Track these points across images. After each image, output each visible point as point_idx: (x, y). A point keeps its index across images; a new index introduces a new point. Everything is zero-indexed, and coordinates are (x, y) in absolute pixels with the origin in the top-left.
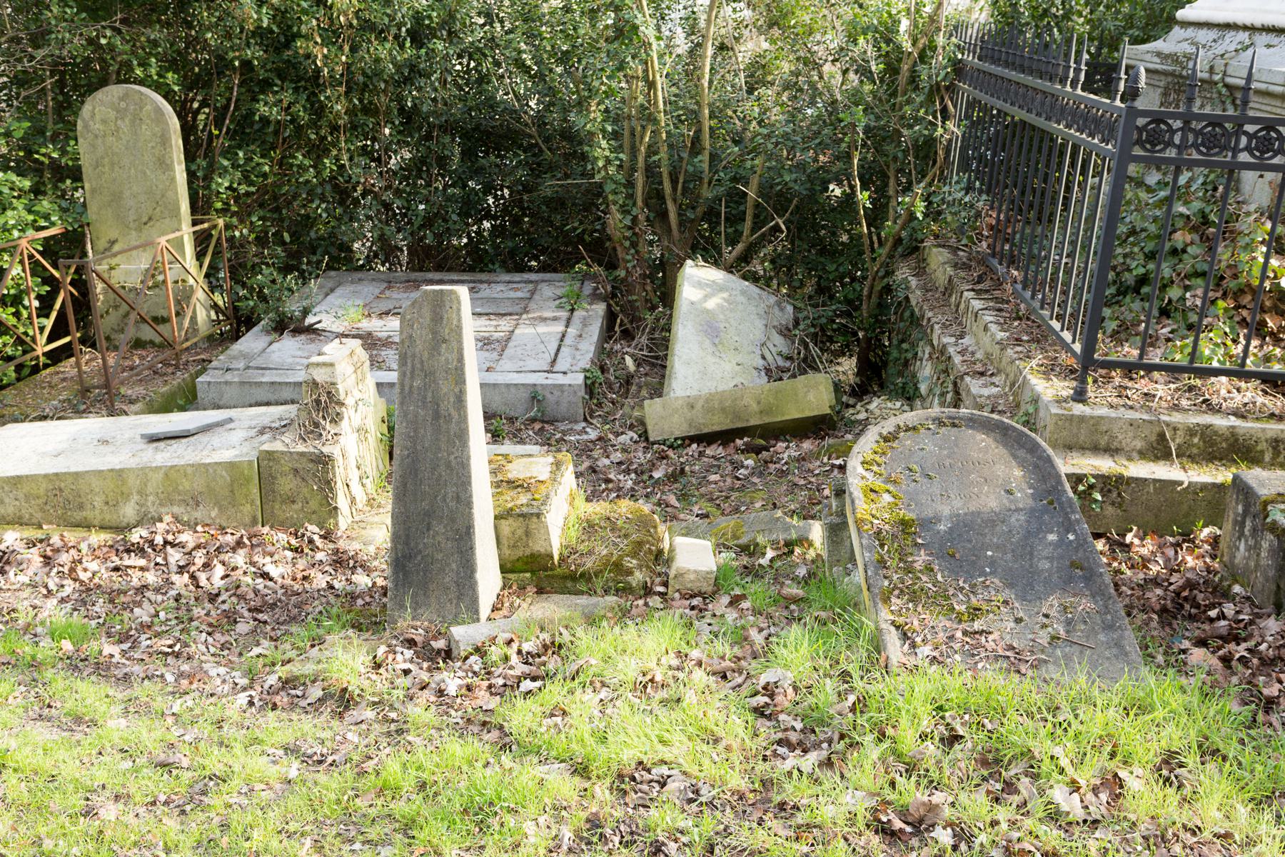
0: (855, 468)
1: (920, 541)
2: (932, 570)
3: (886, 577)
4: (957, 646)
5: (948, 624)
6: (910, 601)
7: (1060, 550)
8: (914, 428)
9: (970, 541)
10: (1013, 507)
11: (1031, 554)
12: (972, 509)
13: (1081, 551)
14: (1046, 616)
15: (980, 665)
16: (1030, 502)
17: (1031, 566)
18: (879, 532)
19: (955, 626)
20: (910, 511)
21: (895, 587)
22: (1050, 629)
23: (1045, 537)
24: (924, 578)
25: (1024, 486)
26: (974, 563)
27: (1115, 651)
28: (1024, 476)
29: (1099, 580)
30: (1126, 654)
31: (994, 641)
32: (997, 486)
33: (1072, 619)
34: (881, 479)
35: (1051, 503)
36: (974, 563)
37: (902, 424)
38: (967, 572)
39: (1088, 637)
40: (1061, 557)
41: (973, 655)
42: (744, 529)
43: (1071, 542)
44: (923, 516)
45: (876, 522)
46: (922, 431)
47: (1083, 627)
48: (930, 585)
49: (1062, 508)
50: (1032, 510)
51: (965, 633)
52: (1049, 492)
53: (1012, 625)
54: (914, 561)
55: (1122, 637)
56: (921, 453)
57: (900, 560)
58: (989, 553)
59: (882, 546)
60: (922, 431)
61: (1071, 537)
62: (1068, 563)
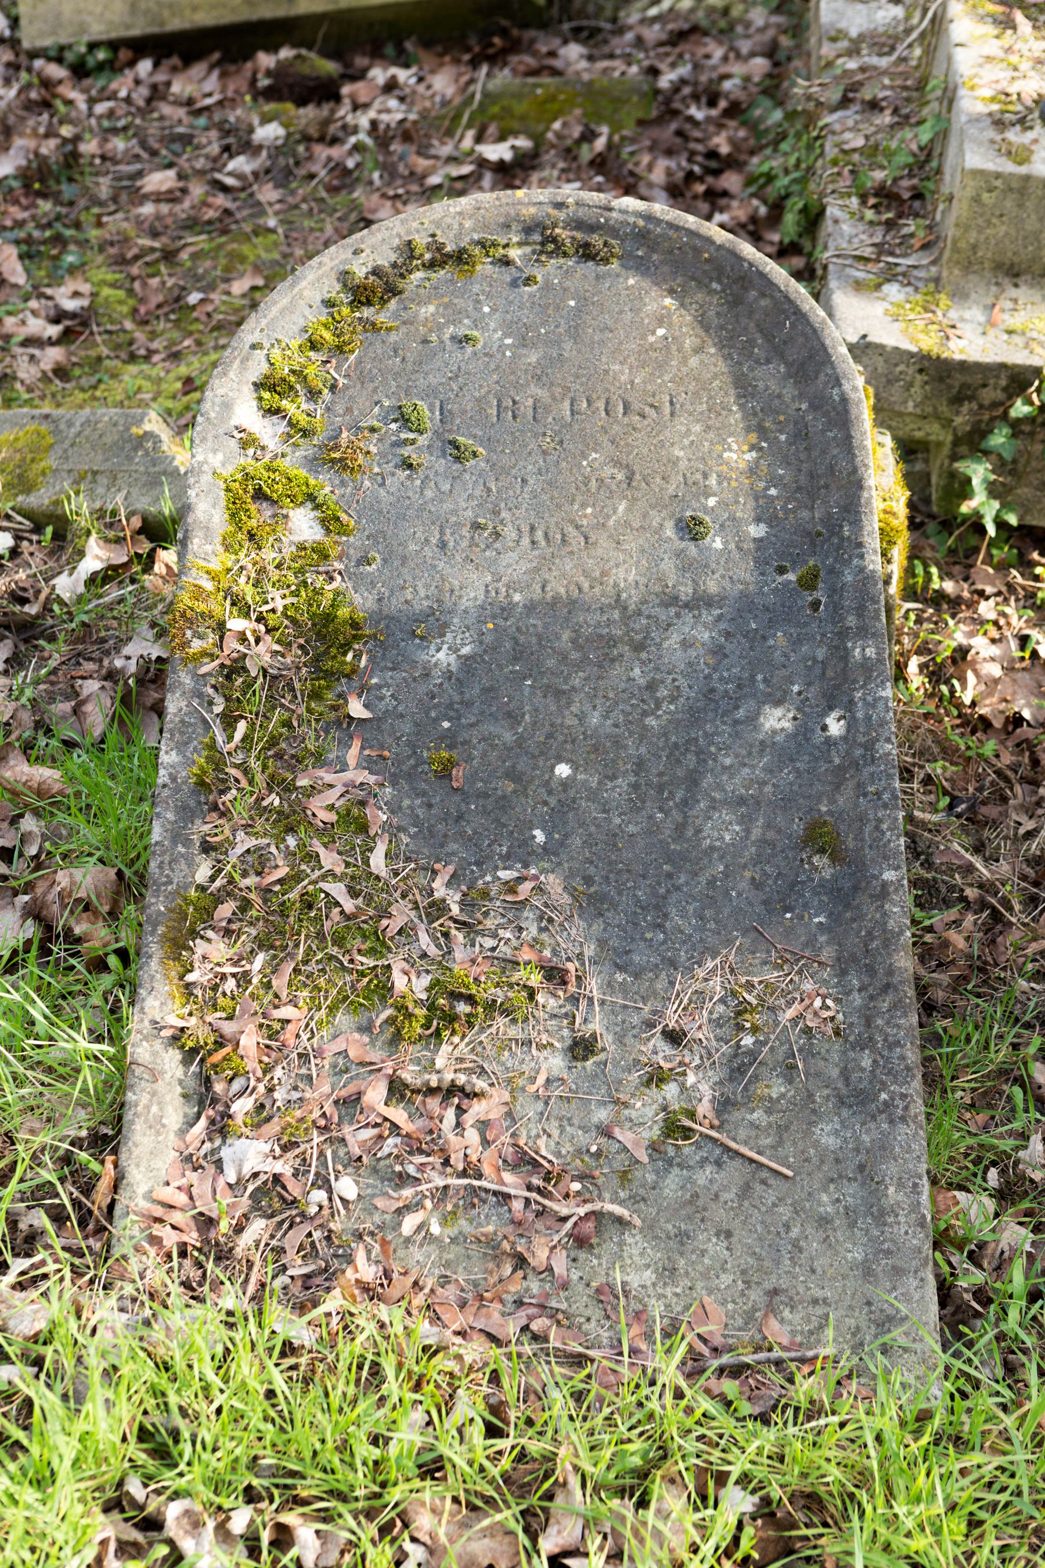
0: (227, 406)
1: (356, 708)
2: (363, 828)
3: (207, 848)
4: (357, 1138)
5: (356, 1045)
6: (262, 943)
7: (787, 775)
8: (460, 258)
9: (513, 718)
10: (686, 591)
11: (693, 781)
12: (558, 588)
13: (849, 788)
14: (674, 1037)
15: (409, 1224)
16: (745, 572)
17: (680, 828)
18: (235, 668)
19: (375, 1055)
20: (358, 580)
21: (228, 892)
22: (671, 1090)
23: (752, 719)
24: (330, 860)
25: (744, 510)
26: (504, 803)
27: (851, 1193)
28: (752, 471)
29: (871, 911)
30: (881, 1216)
31: (483, 1126)
32: (657, 505)
33: (753, 1054)
34: (306, 449)
35: (808, 582)
36: (504, 803)
37: (421, 240)
38: (471, 841)
39: (782, 1129)
40: (786, 802)
41: (403, 1179)
42: (50, 461)
43: (830, 742)
44: (395, 605)
45: (236, 624)
46: (484, 268)
47: (777, 1088)
48: (337, 890)
49: (836, 609)
50: (746, 605)
51: (397, 1090)
52: (813, 538)
53: (555, 1063)
54: (312, 790)
55: (883, 1147)
56: (457, 357)
57: (274, 783)
58: (563, 770)
59: (229, 721)
60: (484, 268)
61: (835, 727)
62: (798, 827)
